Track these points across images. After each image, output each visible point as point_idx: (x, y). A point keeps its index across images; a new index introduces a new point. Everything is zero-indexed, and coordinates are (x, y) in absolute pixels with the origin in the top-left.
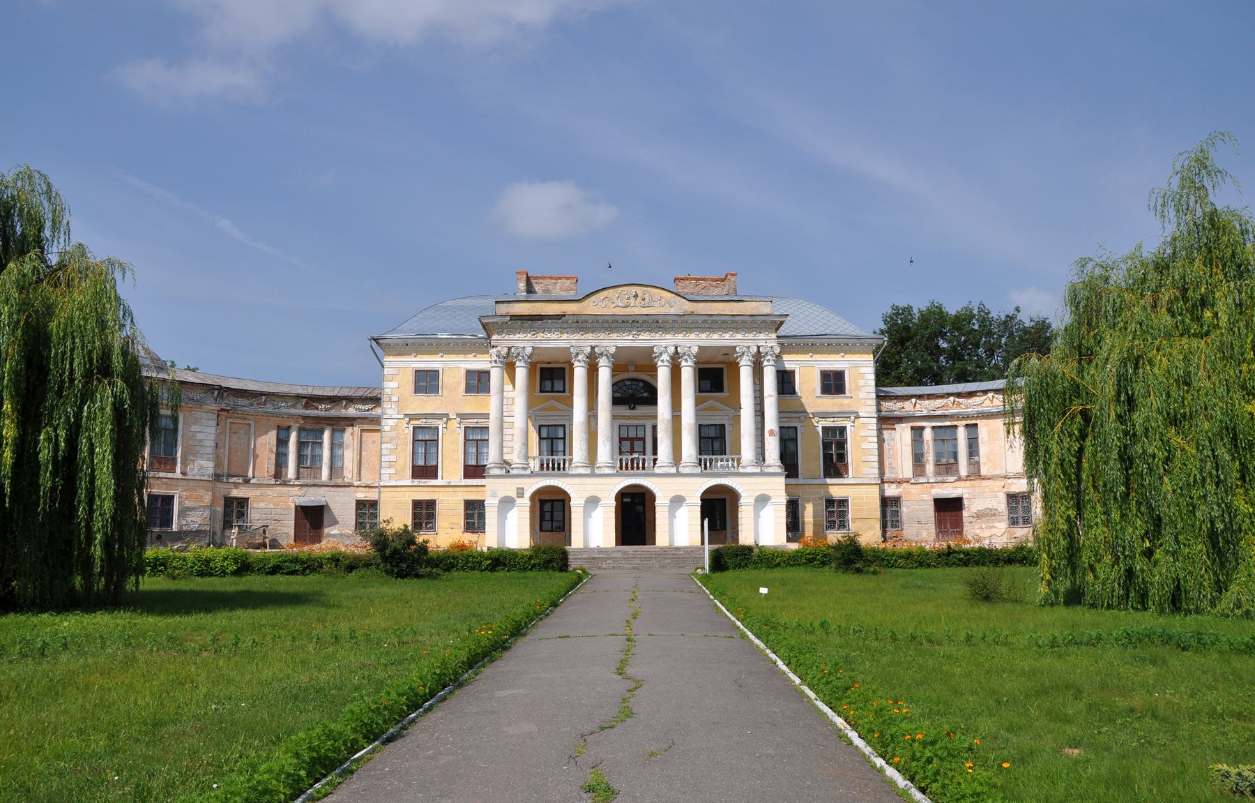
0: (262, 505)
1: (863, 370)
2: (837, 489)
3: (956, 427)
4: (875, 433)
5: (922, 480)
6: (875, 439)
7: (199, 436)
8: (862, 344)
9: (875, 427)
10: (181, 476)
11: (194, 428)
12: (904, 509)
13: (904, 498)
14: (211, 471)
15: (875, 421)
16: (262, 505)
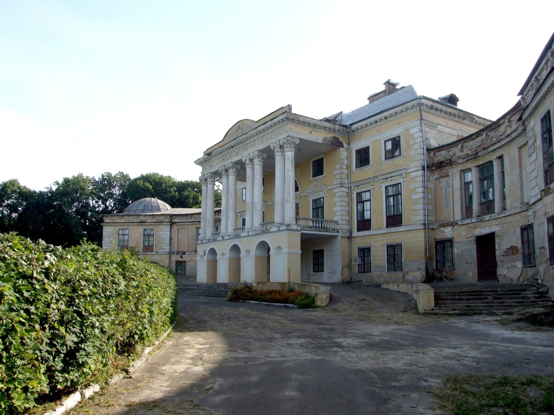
0: (191, 264)
1: (412, 131)
2: (396, 235)
3: (491, 162)
4: (421, 184)
5: (467, 221)
6: (421, 190)
7: (163, 236)
8: (407, 109)
9: (421, 179)
10: (155, 253)
11: (160, 233)
12: (456, 251)
13: (455, 240)
14: (168, 250)
15: (420, 173)
16: (191, 264)
